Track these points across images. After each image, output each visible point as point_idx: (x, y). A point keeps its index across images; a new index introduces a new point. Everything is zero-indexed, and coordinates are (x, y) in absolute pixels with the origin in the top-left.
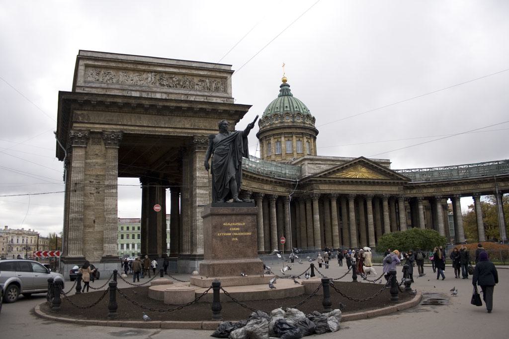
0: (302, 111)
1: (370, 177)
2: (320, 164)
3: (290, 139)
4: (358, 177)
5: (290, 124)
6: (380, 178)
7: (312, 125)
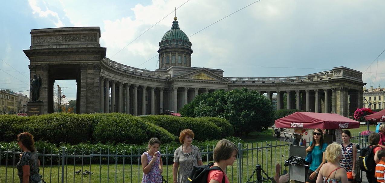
0: (183, 39)
1: (209, 79)
2: (181, 71)
3: (175, 55)
4: (200, 79)
5: (175, 46)
7: (188, 47)
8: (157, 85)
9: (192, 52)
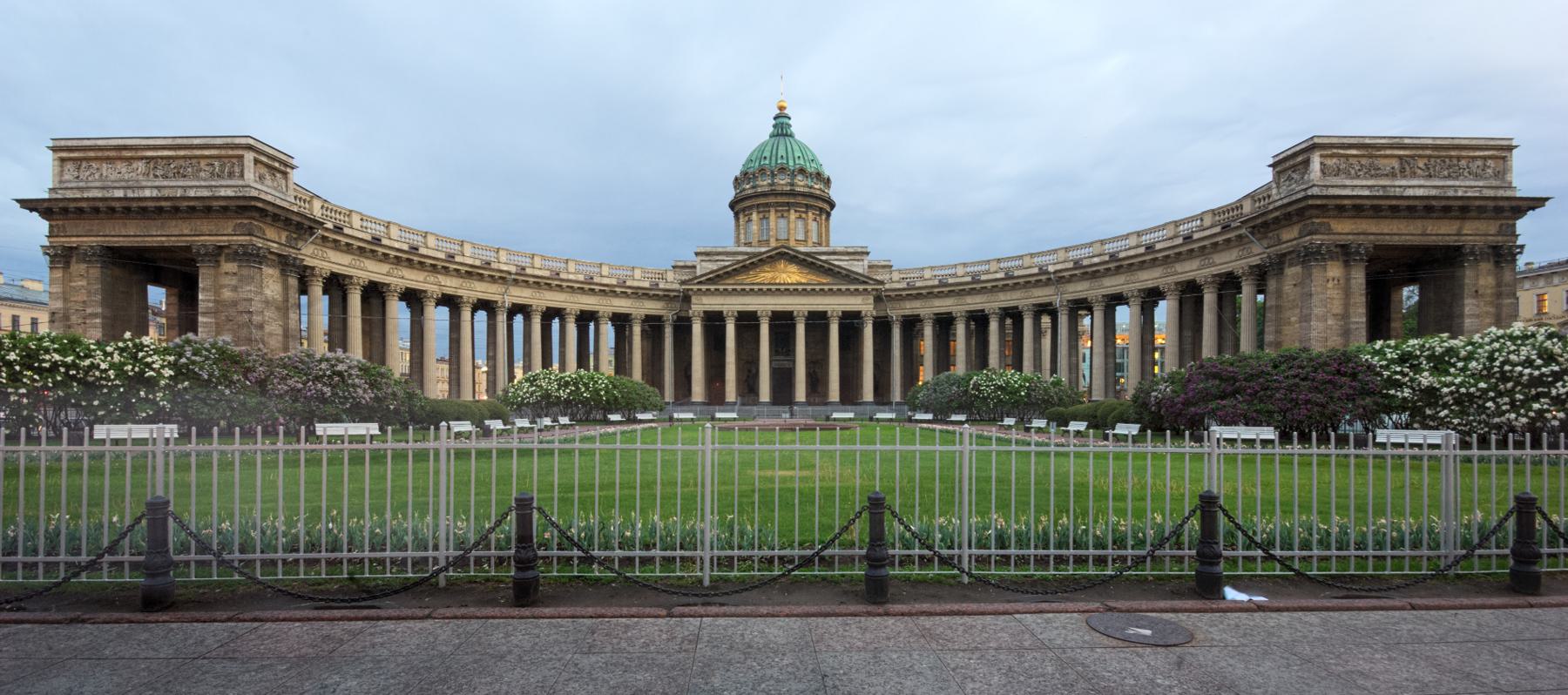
0: (791, 163)
1: (803, 281)
4: (777, 281)
6: (824, 281)
7: (811, 187)
8: (653, 307)
9: (832, 206)
